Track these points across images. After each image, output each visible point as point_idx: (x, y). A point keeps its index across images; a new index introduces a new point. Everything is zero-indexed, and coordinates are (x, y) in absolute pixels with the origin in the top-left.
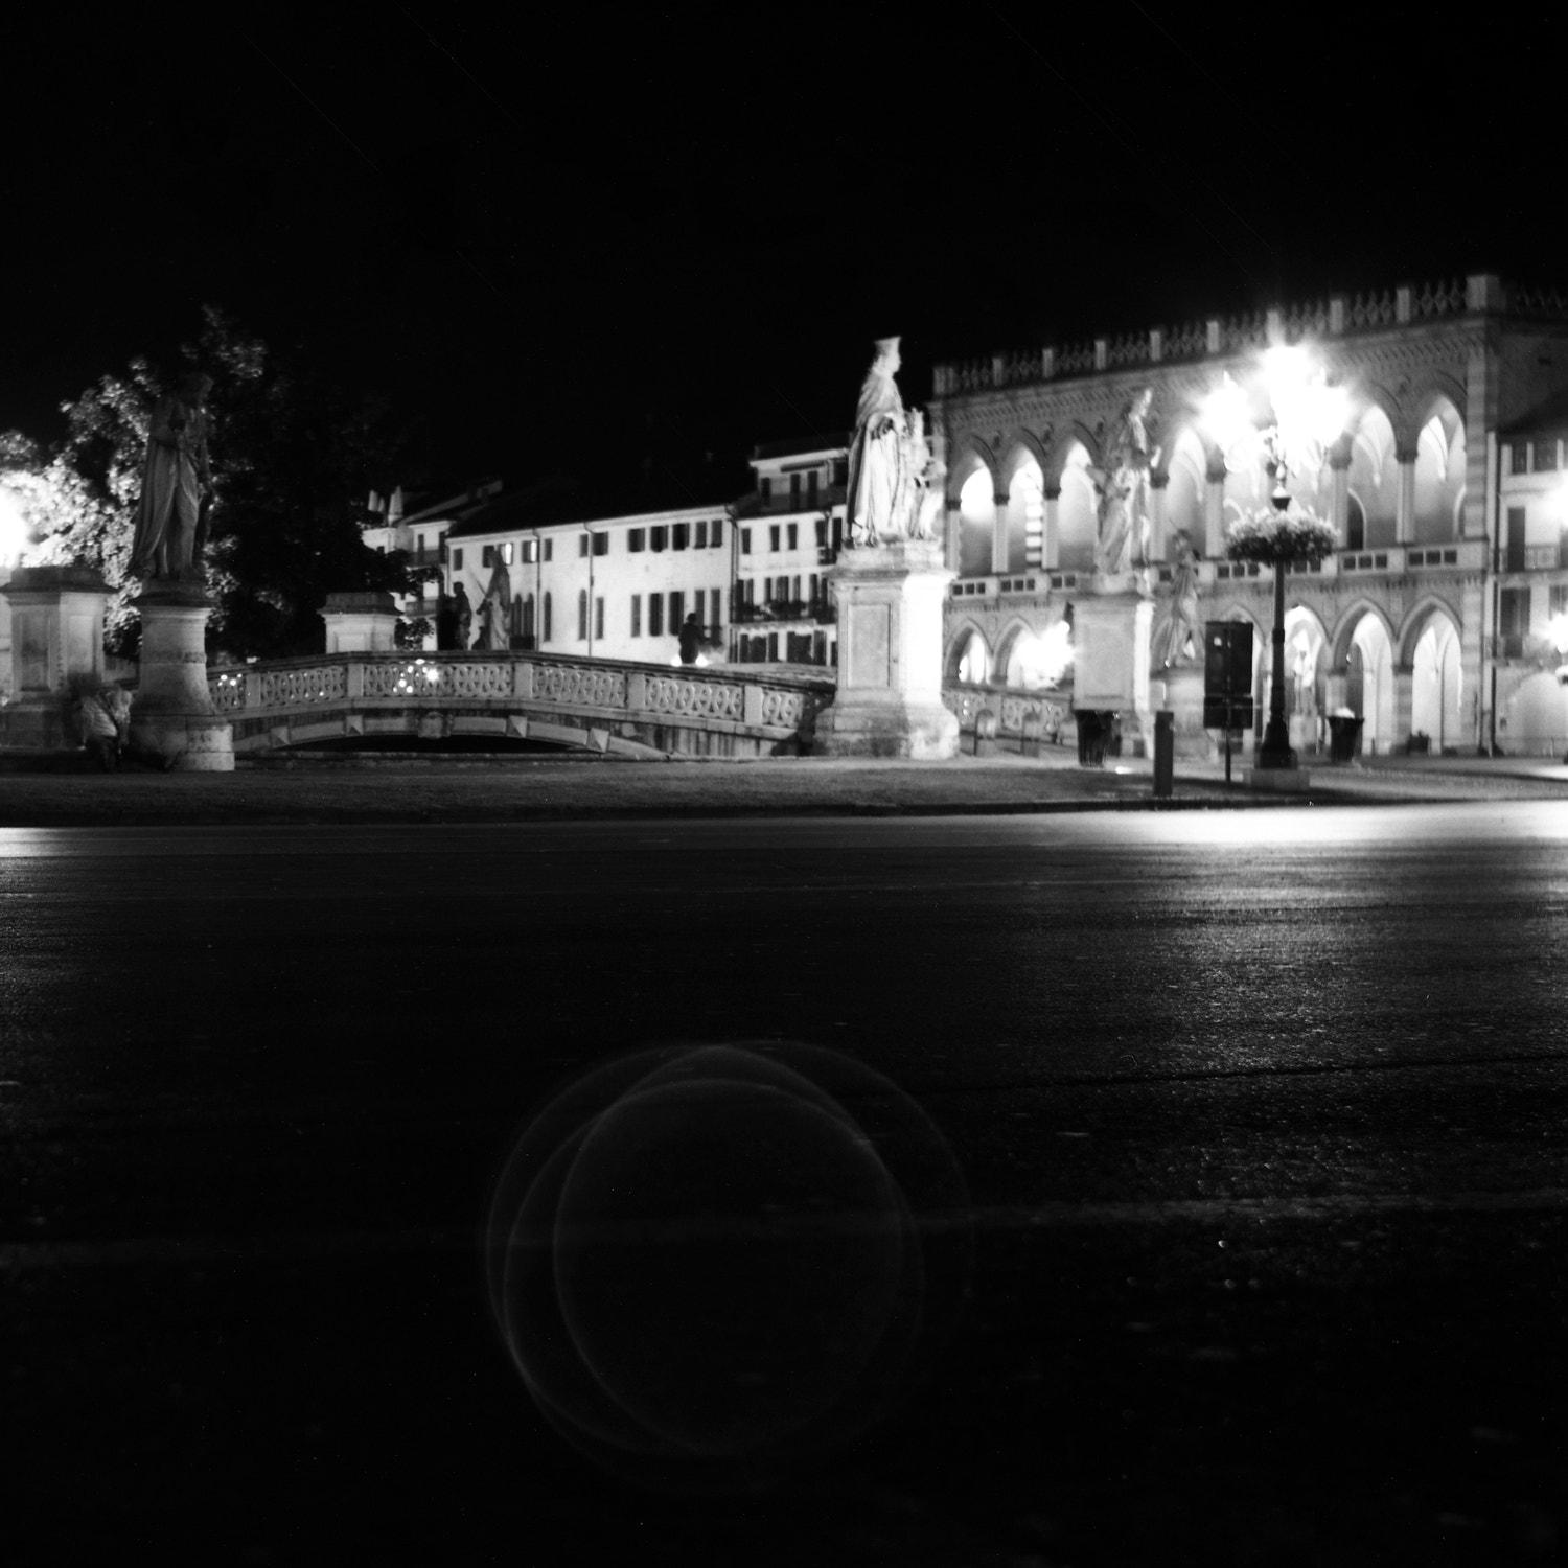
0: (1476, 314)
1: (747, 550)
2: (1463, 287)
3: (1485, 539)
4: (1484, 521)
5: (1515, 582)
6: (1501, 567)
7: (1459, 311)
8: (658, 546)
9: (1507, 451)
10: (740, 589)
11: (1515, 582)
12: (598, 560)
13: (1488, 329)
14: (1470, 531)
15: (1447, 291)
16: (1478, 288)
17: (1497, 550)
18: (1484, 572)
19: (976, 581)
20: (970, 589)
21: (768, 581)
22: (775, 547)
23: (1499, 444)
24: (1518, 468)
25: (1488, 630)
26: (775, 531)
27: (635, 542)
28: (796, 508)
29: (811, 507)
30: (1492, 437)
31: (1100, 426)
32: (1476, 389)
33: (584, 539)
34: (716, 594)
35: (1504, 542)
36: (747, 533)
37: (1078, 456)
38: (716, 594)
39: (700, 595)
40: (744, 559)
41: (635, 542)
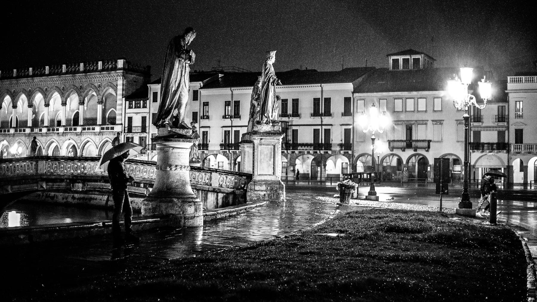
0: (120, 69)
2: (116, 62)
5: (130, 135)
6: (126, 132)
7: (115, 69)
9: (127, 102)
11: (130, 135)
13: (123, 73)
14: (117, 122)
15: (112, 63)
16: (120, 63)
17: (125, 127)
18: (122, 132)
23: (126, 101)
24: (130, 107)
30: (124, 99)
31: (14, 91)
32: (120, 87)
35: (126, 125)
37: (23, 97)
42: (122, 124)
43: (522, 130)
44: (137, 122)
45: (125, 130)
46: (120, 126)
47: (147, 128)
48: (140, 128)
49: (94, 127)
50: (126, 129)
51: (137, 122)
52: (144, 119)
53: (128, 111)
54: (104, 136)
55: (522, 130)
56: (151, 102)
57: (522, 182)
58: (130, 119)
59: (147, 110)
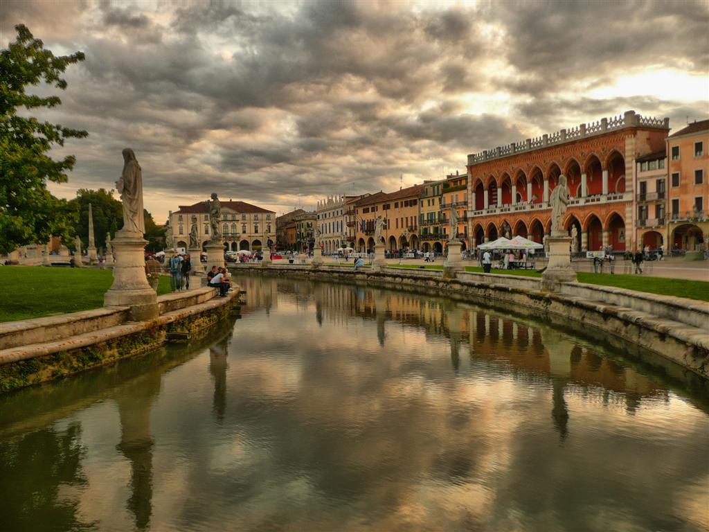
1: (422, 206)
3: (632, 191)
4: (632, 186)
8: (406, 205)
9: (639, 164)
10: (421, 216)
12: (388, 210)
17: (636, 195)
20: (479, 213)
21: (428, 214)
22: (429, 205)
23: (637, 162)
25: (634, 218)
26: (429, 201)
27: (396, 206)
28: (434, 196)
29: (438, 195)
30: (634, 161)
33: (364, 210)
34: (415, 217)
35: (639, 192)
36: (422, 202)
38: (415, 217)
39: (412, 218)
40: (422, 209)
41: (396, 206)
42: (632, 191)
43: (701, 198)
44: (652, 188)
45: (636, 199)
46: (631, 194)
47: (666, 194)
48: (657, 194)
50: (639, 196)
51: (652, 188)
52: (659, 183)
53: (640, 175)
55: (701, 198)
56: (671, 159)
57: (569, 243)
58: (643, 185)
59: (664, 171)
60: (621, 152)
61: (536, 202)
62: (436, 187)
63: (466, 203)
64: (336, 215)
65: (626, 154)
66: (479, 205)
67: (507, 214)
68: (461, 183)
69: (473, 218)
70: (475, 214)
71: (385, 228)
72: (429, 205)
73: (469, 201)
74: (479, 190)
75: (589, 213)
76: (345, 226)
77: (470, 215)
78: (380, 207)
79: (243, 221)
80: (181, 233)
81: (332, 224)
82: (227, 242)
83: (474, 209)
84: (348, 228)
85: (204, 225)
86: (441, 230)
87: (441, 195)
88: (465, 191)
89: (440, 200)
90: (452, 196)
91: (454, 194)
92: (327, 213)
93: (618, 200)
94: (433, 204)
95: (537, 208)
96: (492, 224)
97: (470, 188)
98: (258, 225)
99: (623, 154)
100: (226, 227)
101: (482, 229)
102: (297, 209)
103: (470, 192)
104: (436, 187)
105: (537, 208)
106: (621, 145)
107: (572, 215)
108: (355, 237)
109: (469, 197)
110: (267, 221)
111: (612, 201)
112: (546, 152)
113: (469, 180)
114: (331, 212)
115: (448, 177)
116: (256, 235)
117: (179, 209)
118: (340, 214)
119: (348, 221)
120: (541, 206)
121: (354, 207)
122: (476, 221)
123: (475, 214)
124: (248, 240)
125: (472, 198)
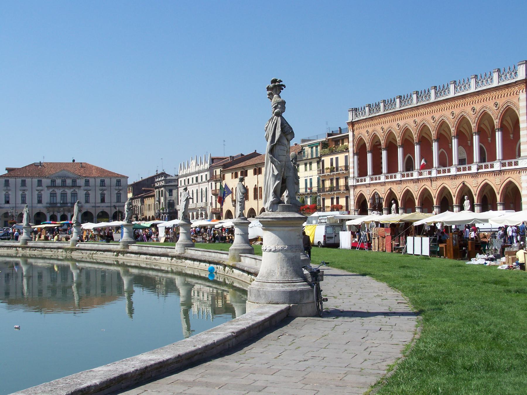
19: (363, 178)
49: (491, 163)
54: (506, 176)
60: (515, 109)
61: (423, 167)
62: (314, 148)
63: (347, 167)
64: (199, 180)
65: (520, 112)
66: (362, 172)
67: (393, 182)
68: (343, 144)
69: (355, 187)
70: (358, 181)
71: (256, 197)
72: (306, 170)
73: (351, 165)
74: (361, 151)
75: (480, 181)
76: (210, 194)
77: (351, 182)
78: (250, 172)
79: (86, 188)
80: (7, 202)
81: (195, 192)
82: (66, 213)
83: (356, 175)
84: (214, 197)
85: (37, 192)
86: (319, 201)
87: (320, 158)
88: (347, 154)
89: (318, 163)
90: (332, 159)
91: (334, 157)
92: (190, 178)
93: (513, 167)
94: (311, 169)
95: (425, 175)
96: (444, 189)
97: (351, 149)
98: (105, 192)
99: (517, 111)
100: (64, 195)
101: (365, 200)
102: (159, 172)
103: (351, 154)
104: (314, 148)
105: (425, 175)
106: (515, 100)
107: (464, 184)
108: (222, 209)
109: (351, 160)
110: (117, 187)
111: (507, 168)
112: (434, 108)
113: (351, 139)
114: (194, 177)
115: (329, 135)
116: (103, 204)
117: (6, 172)
118: (204, 179)
119: (214, 188)
120: (430, 173)
121: (221, 171)
122: (358, 190)
123: (358, 181)
124: (92, 211)
125: (353, 162)
